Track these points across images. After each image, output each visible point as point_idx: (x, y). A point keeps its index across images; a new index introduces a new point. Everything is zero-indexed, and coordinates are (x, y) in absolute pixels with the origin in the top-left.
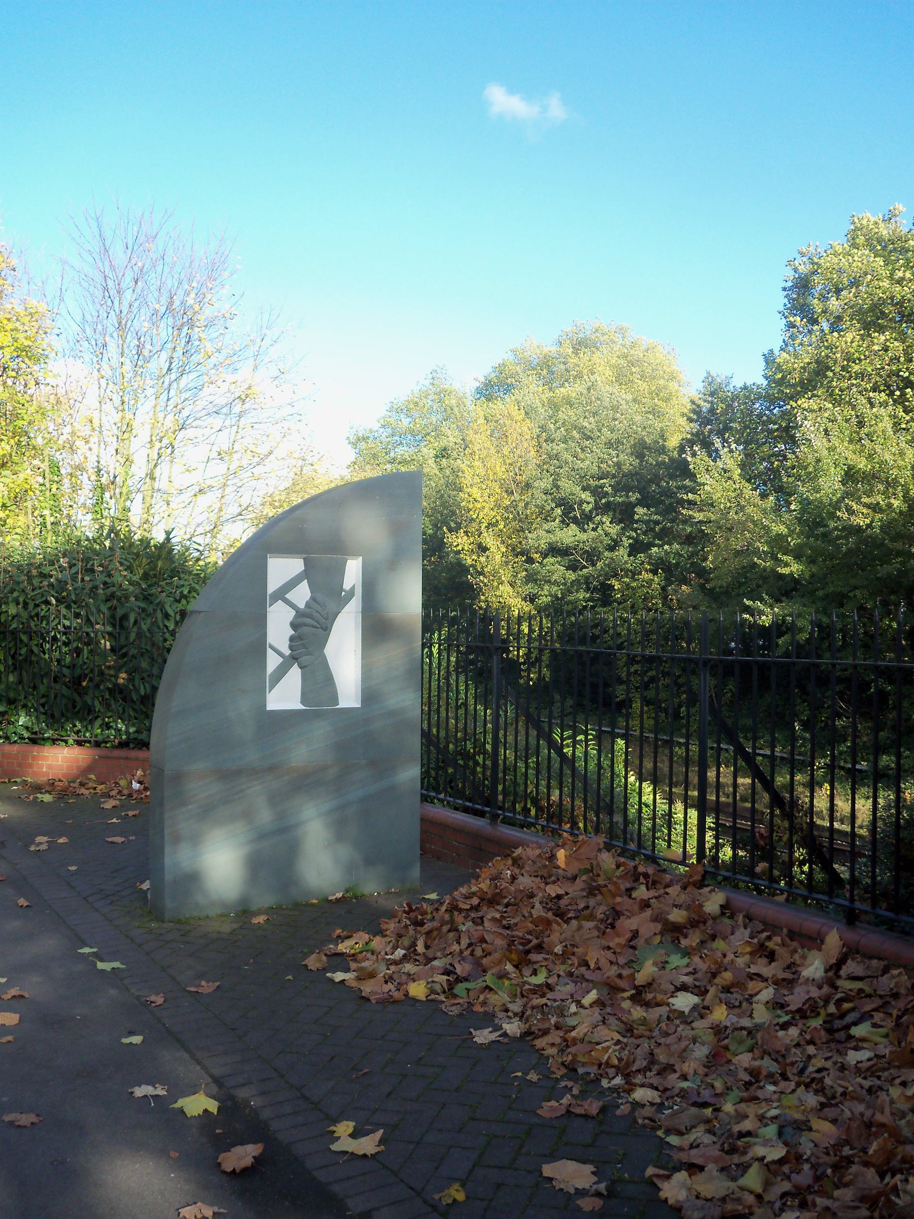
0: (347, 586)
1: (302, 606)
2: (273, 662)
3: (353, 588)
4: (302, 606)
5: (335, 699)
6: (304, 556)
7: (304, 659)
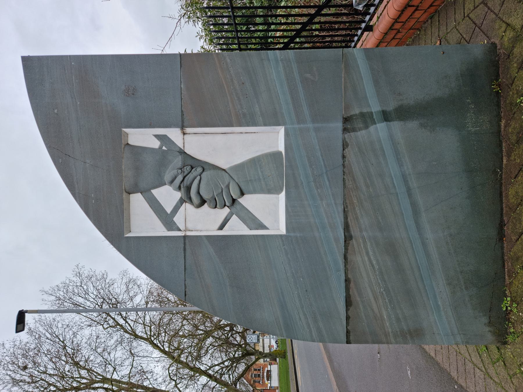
0: (156, 144)
1: (178, 195)
2: (237, 228)
3: (157, 136)
4: (178, 195)
5: (276, 155)
6: (125, 195)
7: (234, 193)
